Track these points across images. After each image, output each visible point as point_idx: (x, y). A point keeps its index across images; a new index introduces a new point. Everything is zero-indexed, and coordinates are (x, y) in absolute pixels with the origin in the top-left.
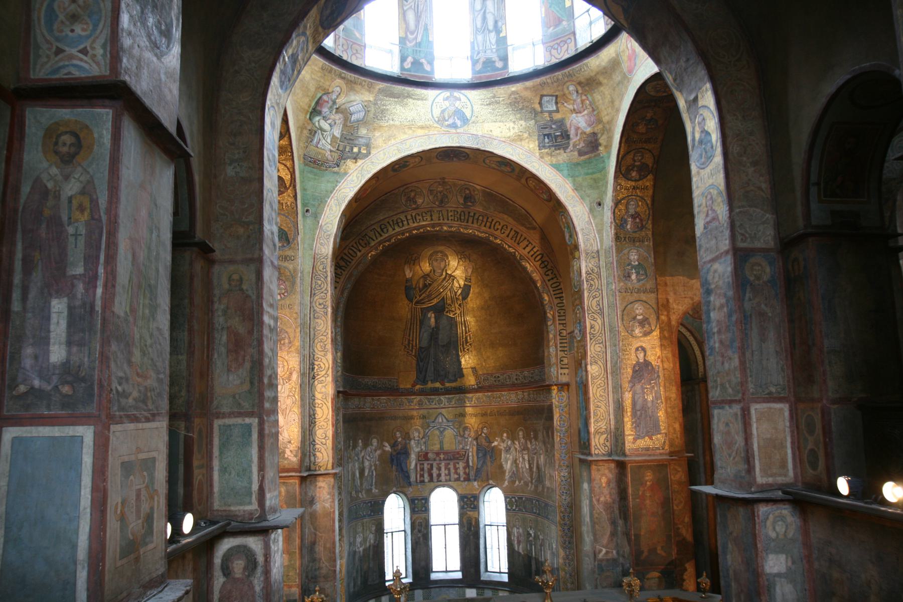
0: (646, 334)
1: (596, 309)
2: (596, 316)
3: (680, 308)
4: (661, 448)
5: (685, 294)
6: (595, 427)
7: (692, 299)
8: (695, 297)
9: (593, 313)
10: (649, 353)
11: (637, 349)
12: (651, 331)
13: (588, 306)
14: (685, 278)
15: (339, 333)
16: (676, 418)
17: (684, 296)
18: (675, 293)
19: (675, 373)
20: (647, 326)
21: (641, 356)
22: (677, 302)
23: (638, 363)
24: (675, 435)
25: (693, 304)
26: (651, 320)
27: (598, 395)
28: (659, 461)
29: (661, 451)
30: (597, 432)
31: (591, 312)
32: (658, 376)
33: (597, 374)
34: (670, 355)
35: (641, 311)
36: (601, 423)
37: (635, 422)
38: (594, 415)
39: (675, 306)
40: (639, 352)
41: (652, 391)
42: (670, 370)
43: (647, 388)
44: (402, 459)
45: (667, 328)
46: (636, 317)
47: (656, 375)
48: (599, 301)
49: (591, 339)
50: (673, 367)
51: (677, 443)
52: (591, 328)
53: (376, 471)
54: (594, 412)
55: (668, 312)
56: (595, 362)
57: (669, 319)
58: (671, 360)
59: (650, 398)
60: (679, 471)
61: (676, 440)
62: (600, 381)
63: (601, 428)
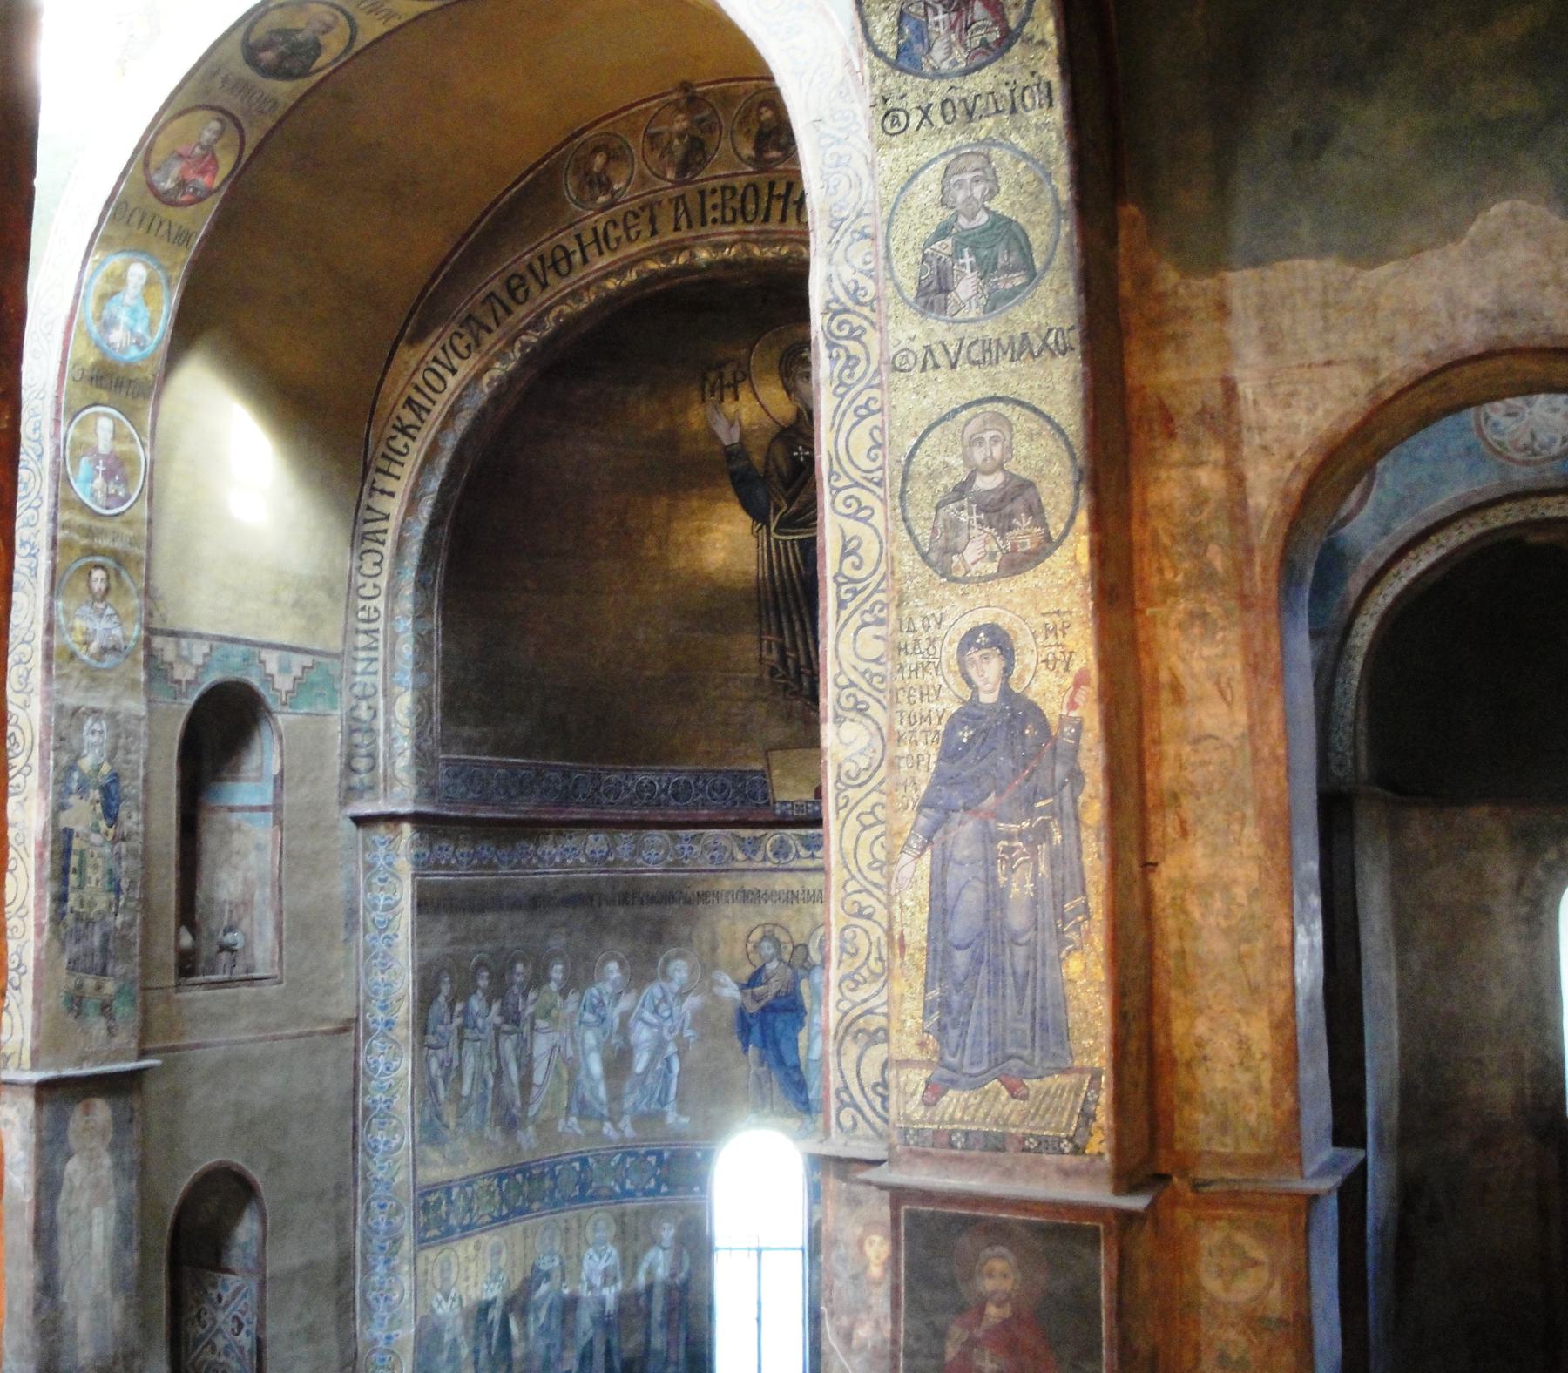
0: (1015, 564)
1: (866, 464)
2: (867, 498)
3: (1301, 417)
4: (1067, 1146)
5: (1327, 347)
6: (846, 1005)
7: (1369, 365)
8: (1384, 353)
9: (857, 484)
10: (1026, 659)
11: (968, 641)
12: (1048, 545)
13: (835, 457)
14: (1330, 264)
15: (410, 634)
16: (1254, 990)
17: (1320, 357)
18: (1271, 349)
19: (1256, 758)
20: (1024, 522)
21: (988, 671)
22: (1282, 389)
23: (970, 713)
24: (1244, 1078)
25: (1374, 392)
26: (1044, 488)
27: (864, 859)
28: (1053, 1207)
29: (1069, 1161)
30: (849, 1029)
31: (844, 482)
32: (1076, 777)
33: (863, 763)
34: (1234, 666)
35: (997, 451)
36: (875, 987)
37: (944, 1005)
38: (843, 950)
39: (1273, 415)
40: (976, 656)
41: (1034, 853)
42: (1229, 739)
43: (1010, 837)
44: (780, 1026)
45: (1222, 529)
46: (971, 479)
47: (1060, 771)
48: (882, 430)
49: (841, 604)
50: (1251, 728)
51: (1252, 1119)
52: (846, 553)
53: (681, 1060)
54: (842, 939)
55: (1233, 446)
56: (855, 708)
57: (1238, 481)
58: (1239, 689)
59: (1020, 887)
60: (1255, 1263)
61: (1252, 1101)
62: (875, 797)
63: (870, 1012)
